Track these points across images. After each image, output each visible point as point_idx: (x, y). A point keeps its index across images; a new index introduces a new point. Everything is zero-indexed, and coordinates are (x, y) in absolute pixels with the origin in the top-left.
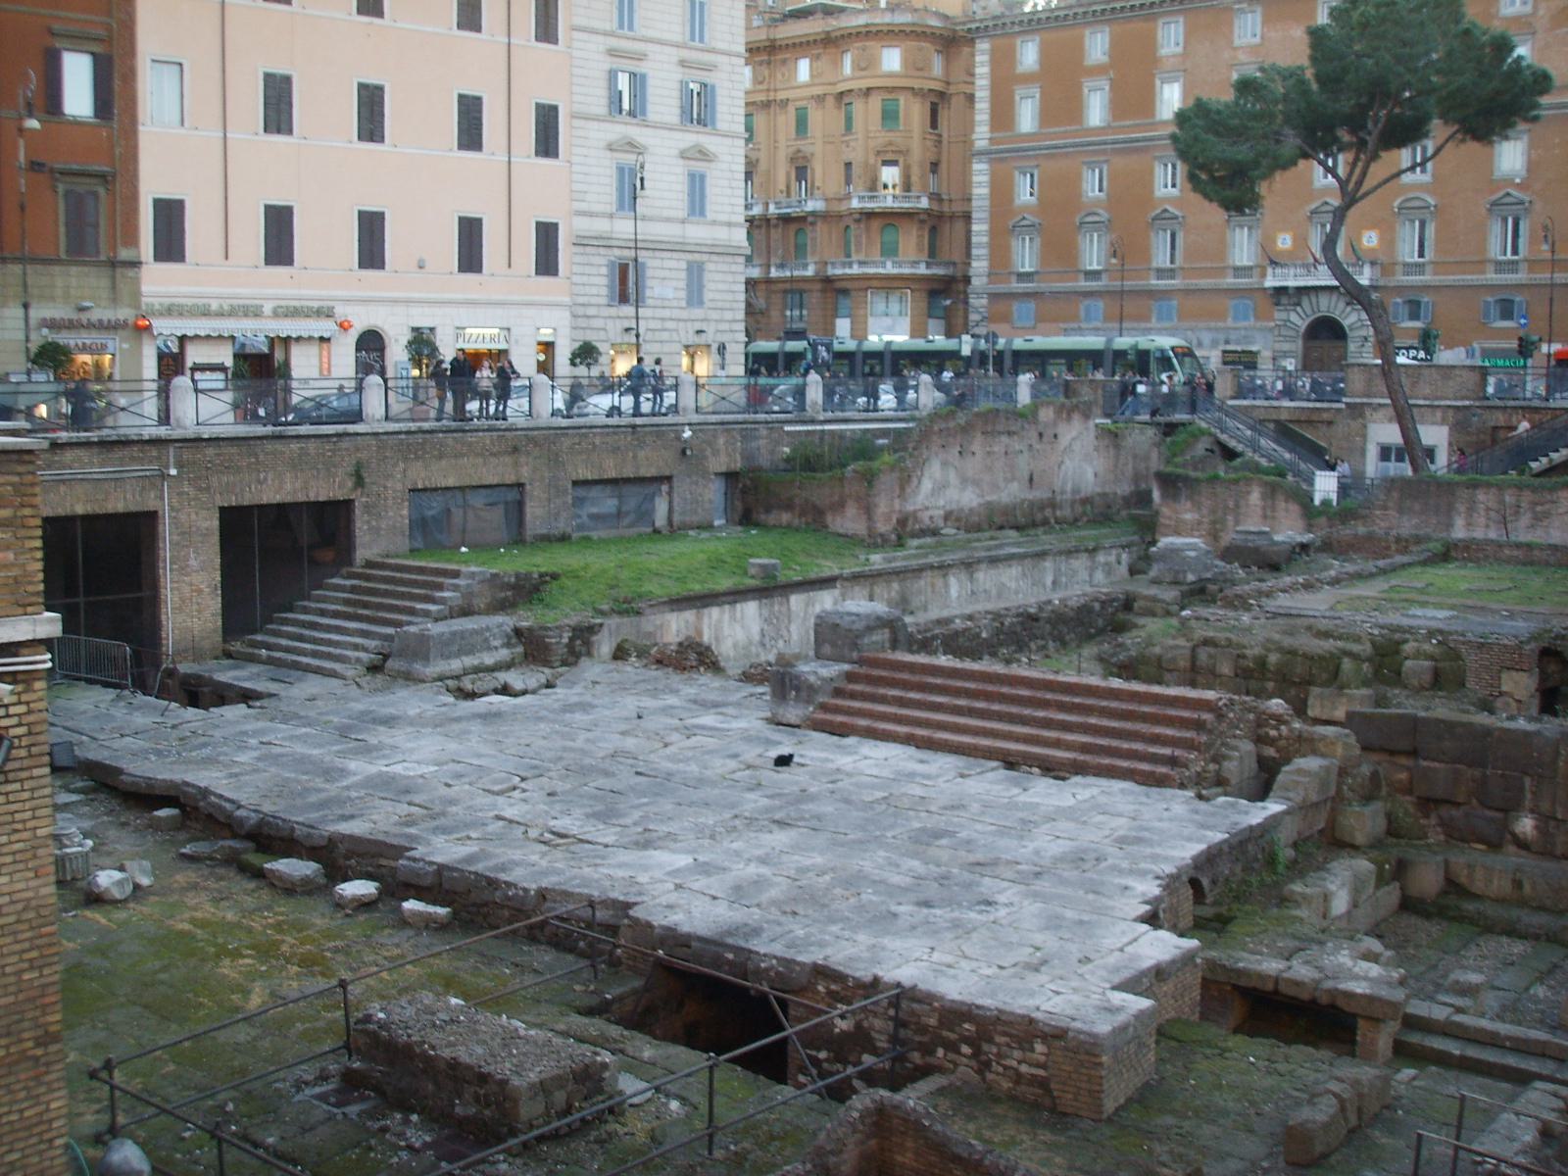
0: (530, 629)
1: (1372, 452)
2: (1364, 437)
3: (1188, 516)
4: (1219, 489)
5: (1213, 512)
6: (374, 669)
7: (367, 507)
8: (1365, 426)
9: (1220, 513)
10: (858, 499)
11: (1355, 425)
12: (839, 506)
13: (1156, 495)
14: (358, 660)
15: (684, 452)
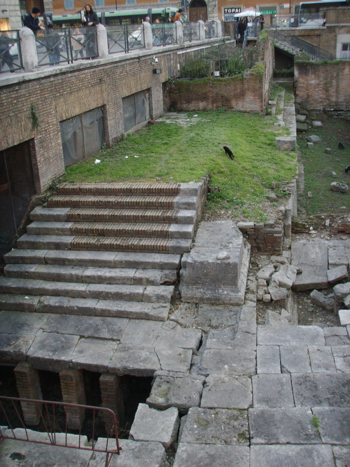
0: (256, 229)
1: (339, 47)
2: (335, 41)
3: (313, 82)
4: (328, 68)
5: (326, 78)
6: (176, 299)
7: (42, 142)
8: (336, 36)
9: (329, 80)
10: (254, 91)
11: (332, 35)
12: (242, 95)
13: (296, 73)
14: (160, 298)
15: (155, 72)
